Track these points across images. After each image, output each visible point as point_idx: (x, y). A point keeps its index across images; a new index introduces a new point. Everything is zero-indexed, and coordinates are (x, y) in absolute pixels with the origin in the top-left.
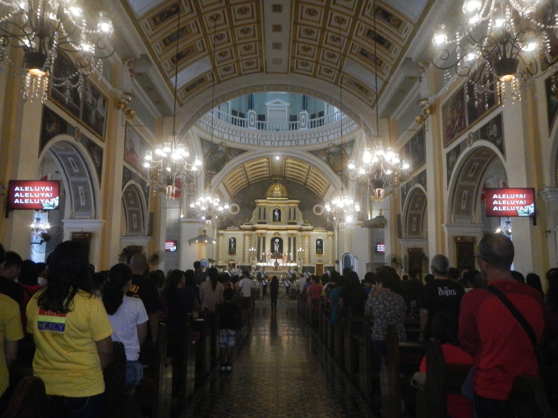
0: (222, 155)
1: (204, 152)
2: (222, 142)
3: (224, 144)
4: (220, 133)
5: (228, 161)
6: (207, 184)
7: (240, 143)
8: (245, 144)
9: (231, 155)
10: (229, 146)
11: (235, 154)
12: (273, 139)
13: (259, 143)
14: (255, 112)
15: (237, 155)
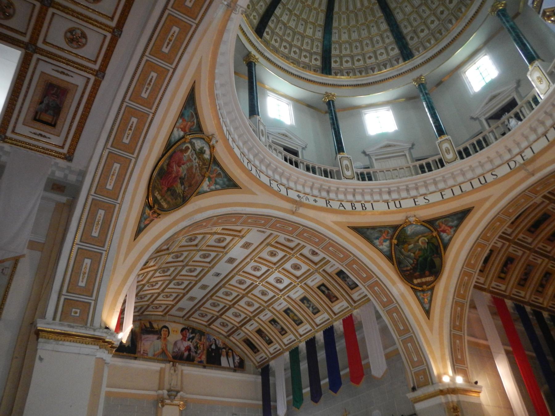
0: (422, 242)
1: (381, 251)
2: (407, 218)
3: (412, 219)
4: (392, 204)
5: (446, 246)
6: (427, 306)
7: (444, 201)
8: (455, 197)
9: (444, 231)
10: (426, 219)
11: (451, 227)
12: (507, 157)
13: (483, 181)
14: (449, 137)
15: (457, 226)
